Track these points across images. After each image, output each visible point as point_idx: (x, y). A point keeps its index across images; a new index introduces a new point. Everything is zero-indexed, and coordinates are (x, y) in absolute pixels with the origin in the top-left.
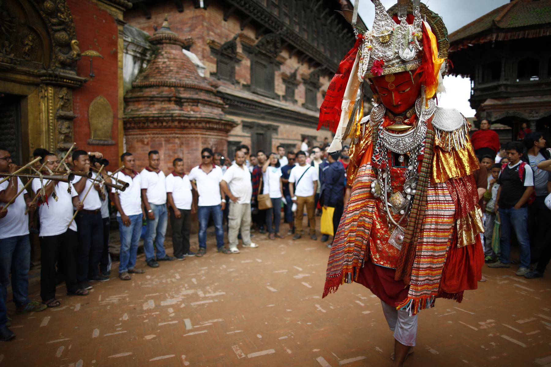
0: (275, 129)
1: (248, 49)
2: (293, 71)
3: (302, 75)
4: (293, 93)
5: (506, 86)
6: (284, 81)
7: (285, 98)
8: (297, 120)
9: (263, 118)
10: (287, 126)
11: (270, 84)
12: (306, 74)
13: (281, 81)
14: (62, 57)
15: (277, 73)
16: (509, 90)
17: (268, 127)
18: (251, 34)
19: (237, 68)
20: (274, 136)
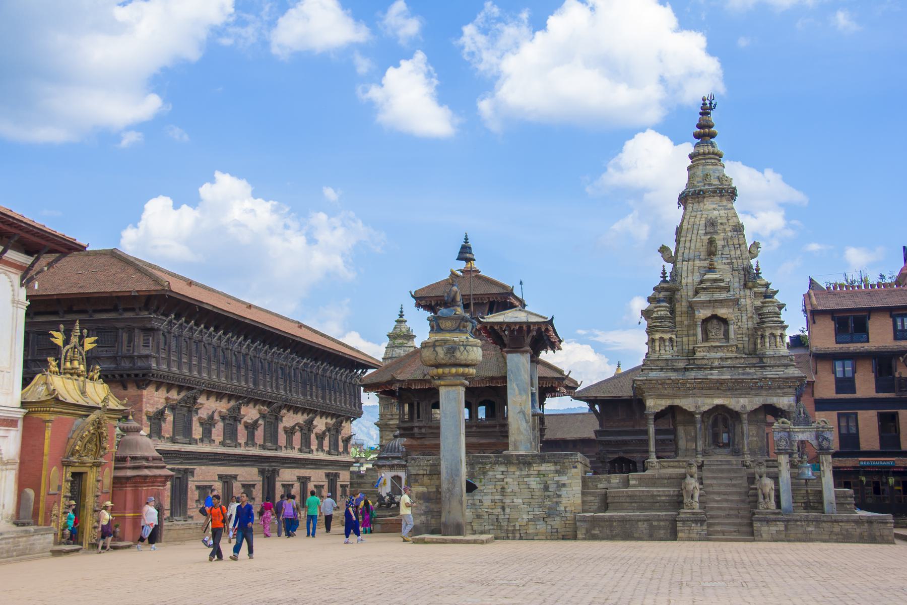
0: (192, 472)
1: (173, 408)
2: (210, 413)
3: (220, 412)
4: (210, 432)
5: (420, 428)
6: (202, 424)
7: (202, 440)
8: (214, 460)
9: (181, 464)
10: (203, 467)
11: (187, 430)
12: (224, 410)
13: (198, 424)
14: (102, 453)
15: (195, 419)
16: (423, 431)
17: (186, 471)
18: (174, 395)
19: (163, 425)
20: (190, 479)
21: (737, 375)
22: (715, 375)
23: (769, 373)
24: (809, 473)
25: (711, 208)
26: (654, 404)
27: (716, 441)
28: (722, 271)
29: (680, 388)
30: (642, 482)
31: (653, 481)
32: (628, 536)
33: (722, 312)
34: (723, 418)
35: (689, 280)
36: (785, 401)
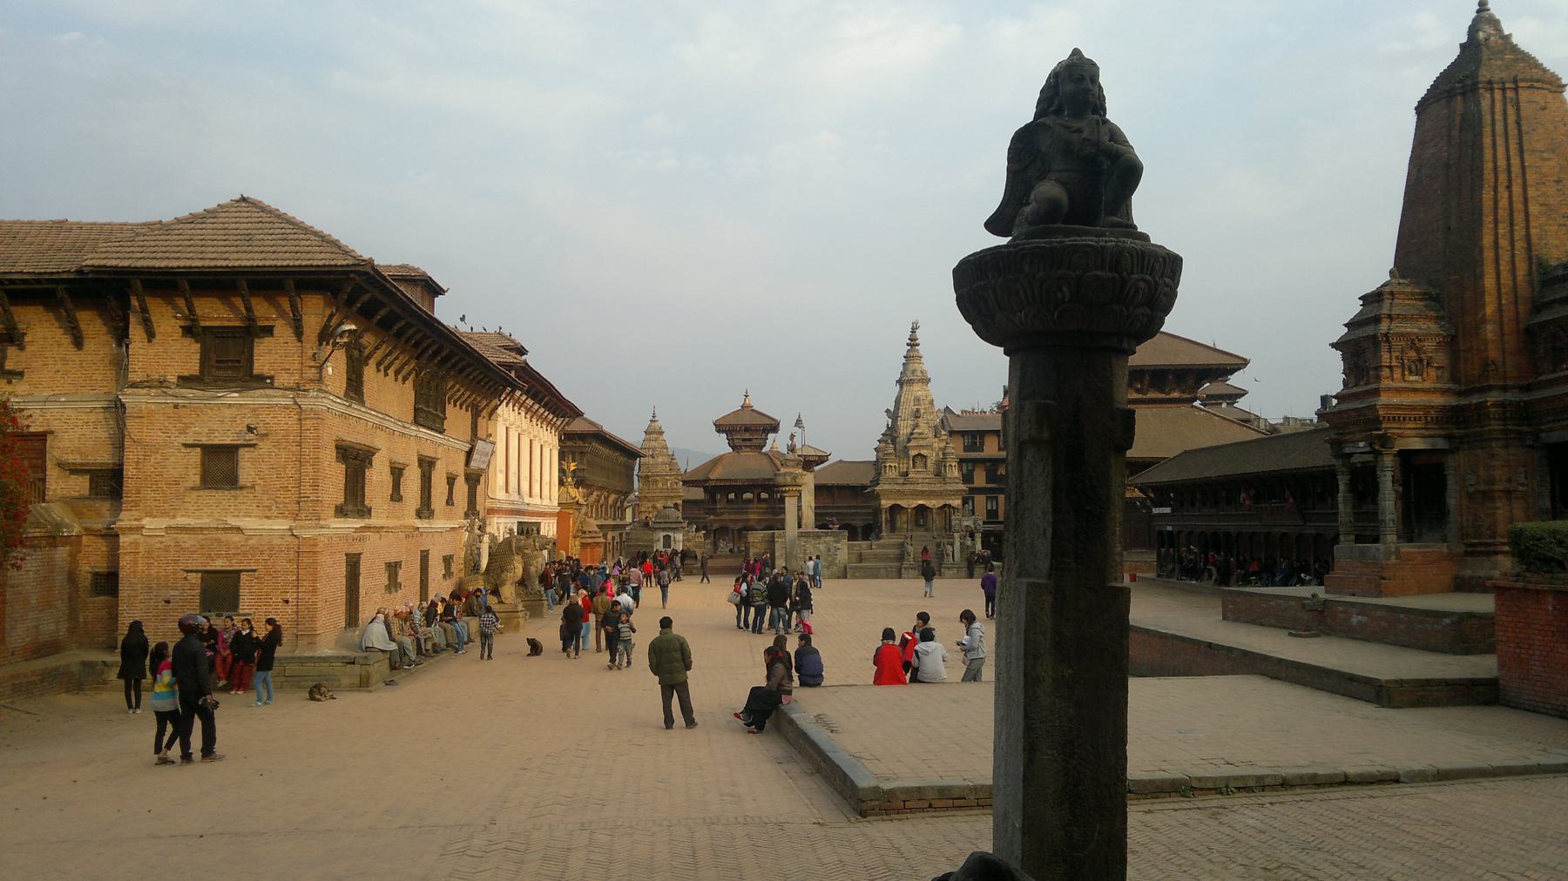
21: (933, 487)
22: (920, 488)
23: (949, 487)
24: (969, 542)
25: (917, 390)
26: (886, 503)
27: (918, 525)
28: (923, 428)
29: (902, 494)
30: (879, 546)
31: (884, 546)
32: (876, 577)
33: (924, 452)
34: (922, 510)
35: (904, 429)
36: (957, 503)
